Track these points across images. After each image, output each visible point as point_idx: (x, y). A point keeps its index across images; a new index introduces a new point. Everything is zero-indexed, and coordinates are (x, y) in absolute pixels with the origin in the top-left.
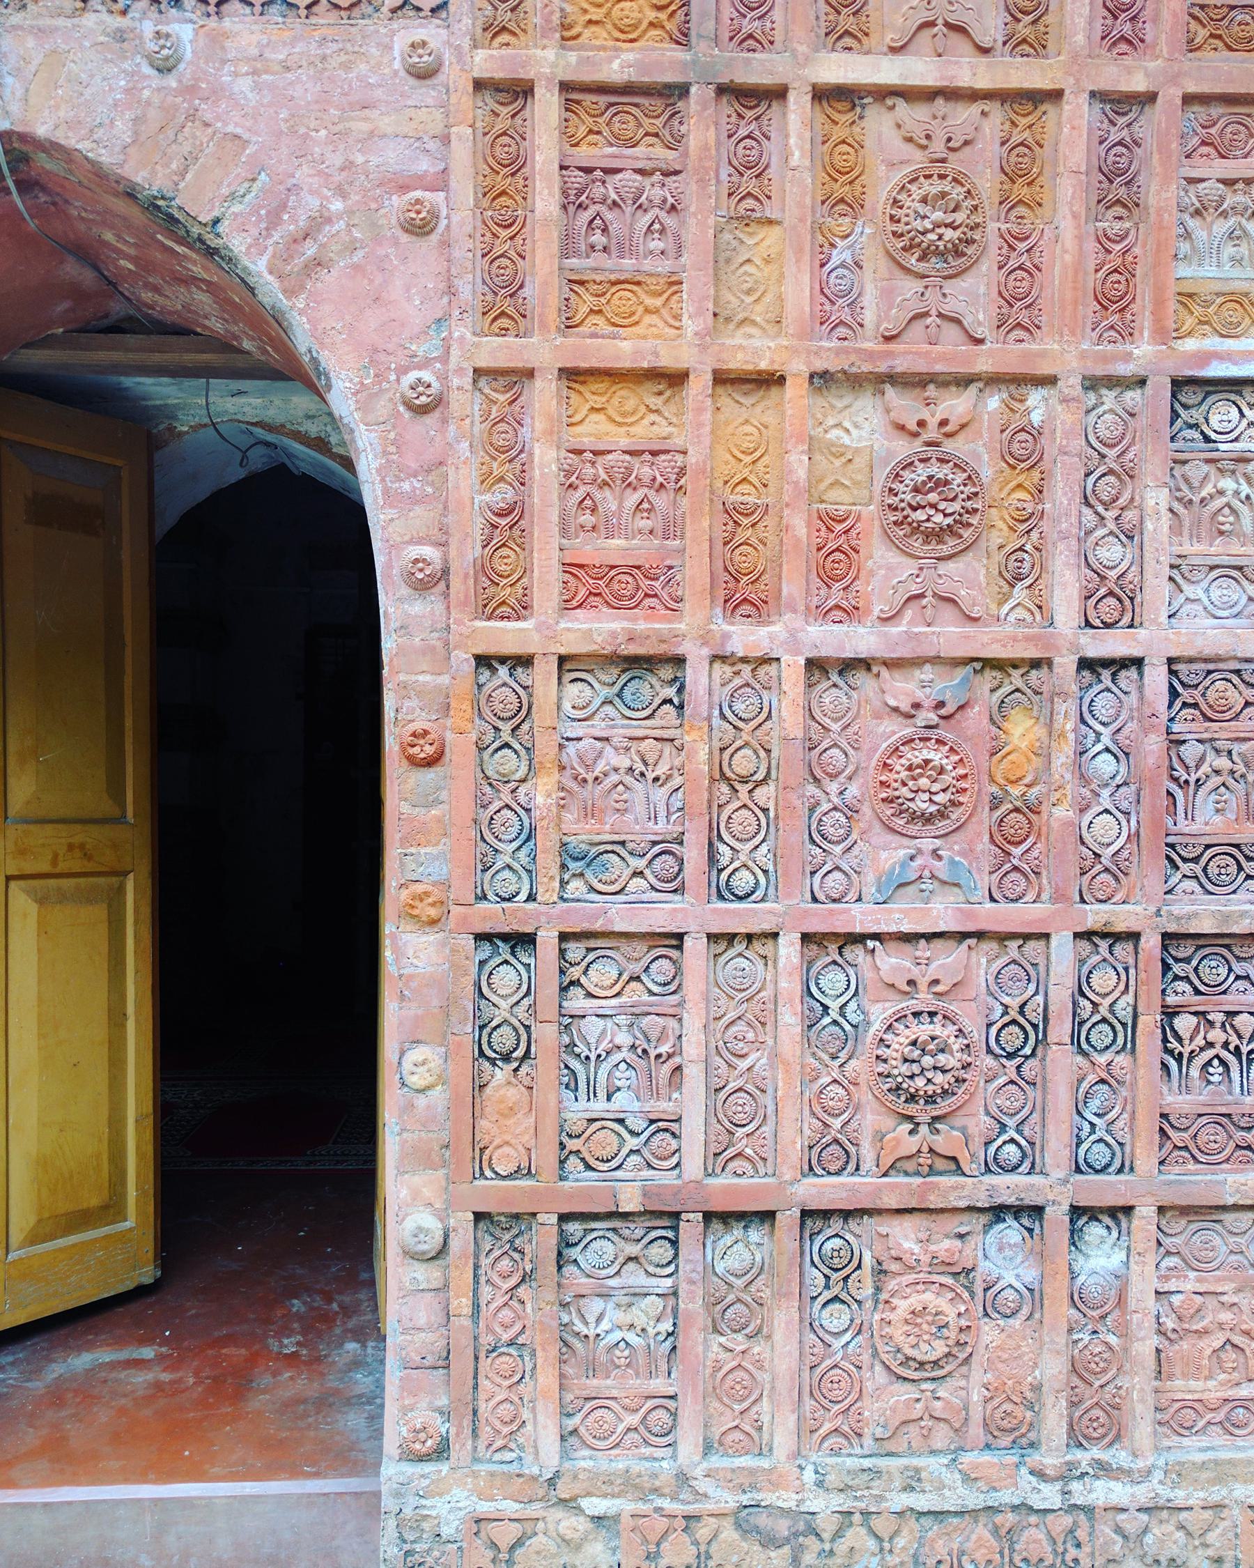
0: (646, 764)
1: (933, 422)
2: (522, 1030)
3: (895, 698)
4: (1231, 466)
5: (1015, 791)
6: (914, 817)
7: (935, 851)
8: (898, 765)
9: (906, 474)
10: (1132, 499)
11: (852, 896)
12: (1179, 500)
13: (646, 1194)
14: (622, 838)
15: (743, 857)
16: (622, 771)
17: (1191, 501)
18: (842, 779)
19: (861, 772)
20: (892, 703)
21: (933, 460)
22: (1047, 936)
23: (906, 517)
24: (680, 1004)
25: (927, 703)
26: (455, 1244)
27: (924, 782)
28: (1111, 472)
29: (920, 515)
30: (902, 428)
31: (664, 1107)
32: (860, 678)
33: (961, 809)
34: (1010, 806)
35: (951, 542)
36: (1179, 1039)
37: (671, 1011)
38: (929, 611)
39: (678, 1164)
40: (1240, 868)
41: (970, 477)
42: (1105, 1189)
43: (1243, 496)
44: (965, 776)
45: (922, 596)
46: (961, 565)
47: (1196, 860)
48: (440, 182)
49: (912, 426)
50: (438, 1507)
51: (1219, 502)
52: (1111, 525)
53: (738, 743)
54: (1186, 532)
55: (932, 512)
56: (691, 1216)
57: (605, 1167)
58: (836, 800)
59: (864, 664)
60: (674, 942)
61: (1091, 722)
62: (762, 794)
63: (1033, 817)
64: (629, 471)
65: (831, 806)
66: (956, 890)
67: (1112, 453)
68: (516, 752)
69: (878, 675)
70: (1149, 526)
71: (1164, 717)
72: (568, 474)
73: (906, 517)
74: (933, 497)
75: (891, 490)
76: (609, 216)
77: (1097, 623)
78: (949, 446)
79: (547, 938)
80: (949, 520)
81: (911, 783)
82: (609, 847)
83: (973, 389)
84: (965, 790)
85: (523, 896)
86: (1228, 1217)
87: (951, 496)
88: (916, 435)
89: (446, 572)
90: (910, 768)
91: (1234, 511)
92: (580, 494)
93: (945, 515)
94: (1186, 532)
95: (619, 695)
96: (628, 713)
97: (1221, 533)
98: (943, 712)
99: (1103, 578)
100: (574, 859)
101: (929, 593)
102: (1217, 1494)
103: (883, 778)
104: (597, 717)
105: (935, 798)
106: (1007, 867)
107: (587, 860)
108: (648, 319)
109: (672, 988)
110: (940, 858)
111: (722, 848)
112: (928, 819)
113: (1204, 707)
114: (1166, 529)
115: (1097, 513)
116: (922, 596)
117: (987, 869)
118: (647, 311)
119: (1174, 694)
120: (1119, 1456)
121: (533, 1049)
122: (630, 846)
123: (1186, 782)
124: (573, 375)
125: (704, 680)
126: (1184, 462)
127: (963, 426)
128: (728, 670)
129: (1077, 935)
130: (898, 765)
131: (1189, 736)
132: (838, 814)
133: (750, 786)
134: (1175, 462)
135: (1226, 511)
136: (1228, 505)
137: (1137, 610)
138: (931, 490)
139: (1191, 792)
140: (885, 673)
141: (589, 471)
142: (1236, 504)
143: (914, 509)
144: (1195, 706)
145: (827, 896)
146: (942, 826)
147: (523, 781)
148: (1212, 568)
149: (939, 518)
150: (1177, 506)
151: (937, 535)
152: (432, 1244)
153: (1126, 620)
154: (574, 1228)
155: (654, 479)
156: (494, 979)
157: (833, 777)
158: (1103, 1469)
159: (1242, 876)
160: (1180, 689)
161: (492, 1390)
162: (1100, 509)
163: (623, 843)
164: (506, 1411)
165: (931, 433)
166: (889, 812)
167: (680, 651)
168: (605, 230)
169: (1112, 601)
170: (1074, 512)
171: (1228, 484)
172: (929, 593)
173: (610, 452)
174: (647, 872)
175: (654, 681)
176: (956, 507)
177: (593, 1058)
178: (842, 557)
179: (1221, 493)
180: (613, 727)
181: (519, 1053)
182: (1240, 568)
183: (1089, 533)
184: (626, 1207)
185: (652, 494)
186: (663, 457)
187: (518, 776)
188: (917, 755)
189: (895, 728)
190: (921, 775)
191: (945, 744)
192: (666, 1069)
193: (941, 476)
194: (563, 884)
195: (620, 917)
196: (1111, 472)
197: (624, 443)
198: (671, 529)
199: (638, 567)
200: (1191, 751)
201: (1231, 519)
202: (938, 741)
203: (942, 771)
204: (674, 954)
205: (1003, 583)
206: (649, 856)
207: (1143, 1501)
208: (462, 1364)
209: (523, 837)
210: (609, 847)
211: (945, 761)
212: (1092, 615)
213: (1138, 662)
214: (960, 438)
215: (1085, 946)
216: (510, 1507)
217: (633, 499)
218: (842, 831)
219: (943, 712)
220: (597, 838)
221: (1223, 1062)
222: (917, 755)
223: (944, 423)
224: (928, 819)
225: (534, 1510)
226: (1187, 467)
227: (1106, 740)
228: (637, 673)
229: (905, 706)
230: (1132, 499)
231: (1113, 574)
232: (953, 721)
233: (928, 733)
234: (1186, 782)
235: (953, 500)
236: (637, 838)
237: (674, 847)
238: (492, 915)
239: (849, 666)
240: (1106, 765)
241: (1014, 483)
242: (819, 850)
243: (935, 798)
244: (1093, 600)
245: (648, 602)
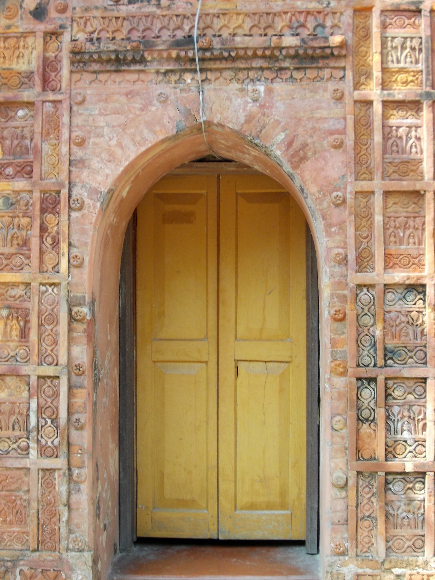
2: (372, 411)
13: (415, 466)
24: (426, 402)
26: (350, 482)
31: (420, 436)
37: (423, 404)
39: (425, 456)
48: (343, 132)
50: (345, 570)
56: (430, 473)
57: (401, 456)
60: (423, 381)
68: (369, 316)
76: (398, 141)
79: (381, 379)
82: (401, 348)
85: (372, 365)
89: (346, 256)
95: (404, 297)
100: (389, 354)
108: (412, 174)
109: (423, 396)
118: (412, 171)
121: (376, 416)
122: (408, 348)
124: (387, 194)
152: (342, 482)
154: (390, 477)
156: (363, 393)
161: (363, 534)
164: (366, 540)
167: (424, 282)
168: (397, 146)
173: (400, 217)
174: (414, 357)
177: (396, 420)
181: (371, 418)
184: (407, 470)
187: (370, 324)
192: (421, 424)
194: (386, 361)
195: (406, 373)
197: (404, 214)
199: (410, 255)
204: (423, 385)
206: (415, 351)
208: (352, 523)
210: (401, 348)
216: (369, 571)
220: (397, 345)
225: (377, 572)
237: (423, 349)
238: (363, 372)
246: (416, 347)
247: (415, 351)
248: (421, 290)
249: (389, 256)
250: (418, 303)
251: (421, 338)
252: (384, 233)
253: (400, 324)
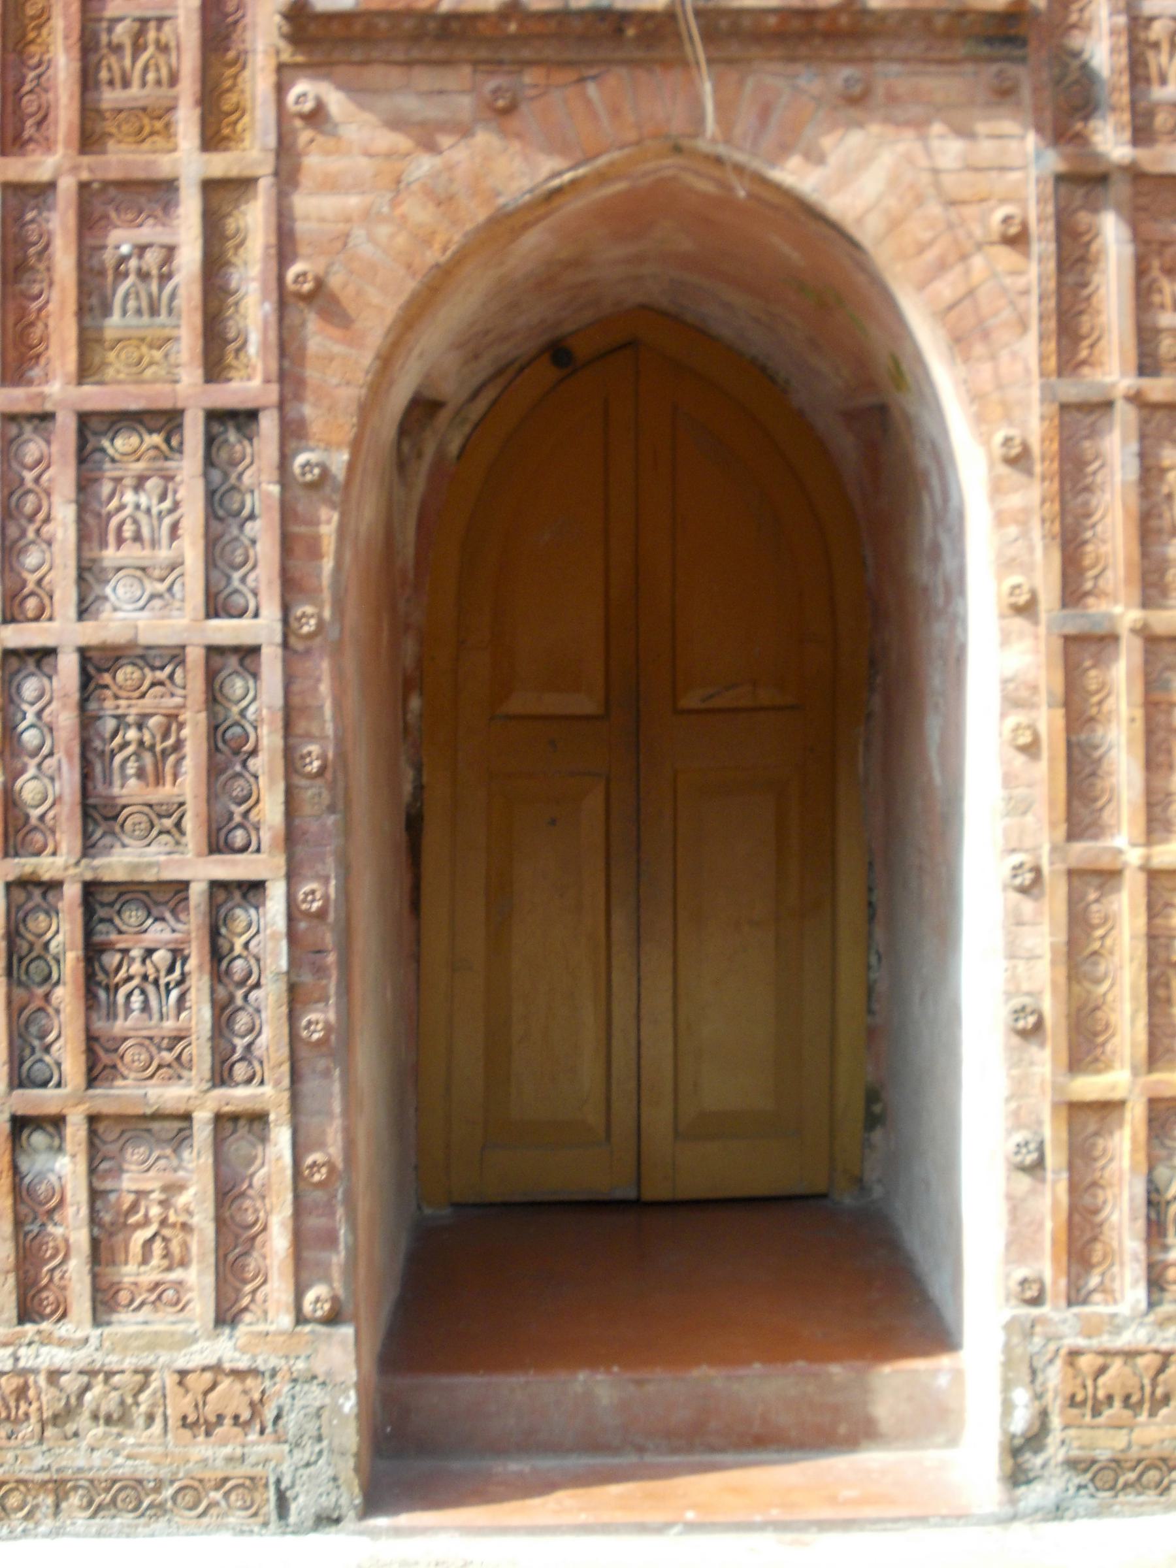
36: (106, 972)
42: (43, 1100)
86: (156, 1126)
102: (146, 1360)
120: (64, 1330)
158: (46, 1340)
182: (143, 569)
207: (82, 1365)
215: (19, 895)
221: (143, 992)
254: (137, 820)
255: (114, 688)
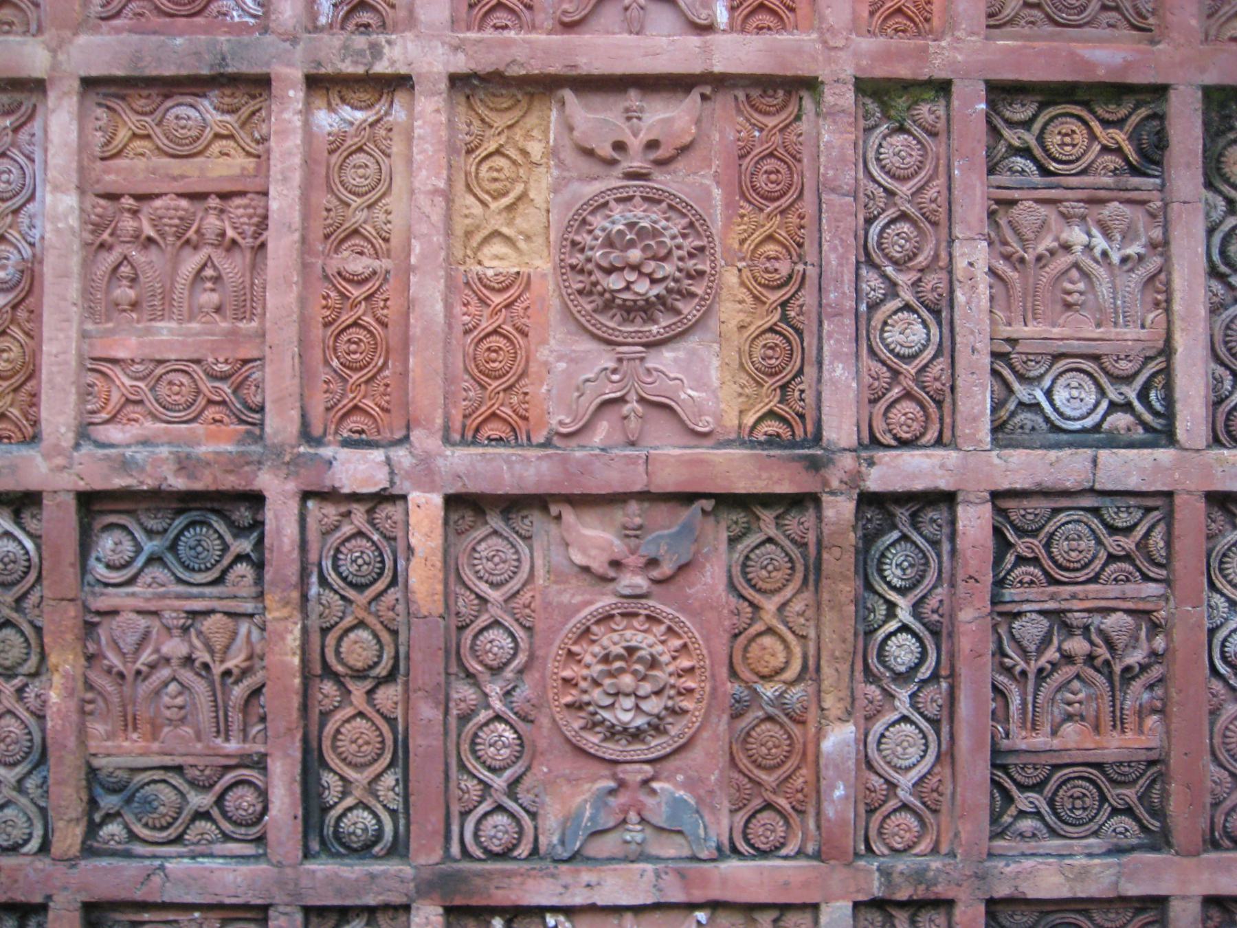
0: (212, 652)
1: (635, 144)
3: (584, 551)
4: (1080, 209)
5: (768, 691)
6: (613, 733)
7: (645, 782)
8: (590, 653)
9: (598, 221)
10: (936, 257)
11: (523, 850)
12: (1007, 258)
14: (178, 761)
15: (358, 793)
16: (174, 662)
17: (1022, 260)
18: (508, 674)
19: (537, 664)
20: (579, 559)
21: (637, 200)
22: (815, 907)
23: (595, 284)
25: (631, 560)
27: (627, 680)
28: (904, 216)
29: (615, 282)
30: (589, 153)
32: (535, 521)
33: (684, 720)
34: (761, 714)
35: (665, 320)
38: (633, 424)
40: (1103, 799)
41: (691, 224)
43: (1097, 252)
44: (691, 670)
45: (622, 400)
46: (681, 354)
47: (1038, 787)
49: (606, 150)
51: (1064, 260)
52: (907, 296)
53: (349, 621)
54: (1017, 305)
55: (632, 277)
58: (498, 705)
59: (539, 502)
61: (881, 587)
62: (388, 696)
63: (796, 730)
64: (186, 222)
65: (490, 713)
66: (679, 839)
67: (904, 189)
69: (558, 518)
70: (960, 297)
71: (989, 578)
72: (97, 228)
73: (595, 284)
74: (635, 255)
75: (574, 244)
77: (888, 439)
78: (663, 180)
80: (658, 289)
81: (607, 682)
82: (158, 775)
83: (695, 95)
84: (690, 691)
85: (34, 844)
87: (663, 252)
88: (612, 163)
90: (606, 659)
91: (1085, 275)
92: (111, 258)
93: (654, 282)
94: (1017, 305)
95: (173, 547)
96: (185, 576)
97: (1068, 306)
98: (655, 574)
99: (896, 373)
101: (633, 397)
103: (567, 673)
104: (140, 581)
105: (645, 706)
106: (757, 803)
107: (126, 793)
110: (653, 792)
111: (328, 778)
112: (637, 735)
113: (1047, 564)
114: (985, 303)
115: (885, 276)
116: (622, 400)
117: (726, 806)
119: (1002, 545)
123: (1024, 673)
125: (291, 530)
126: (1013, 203)
127: (684, 149)
128: (331, 511)
129: (857, 905)
130: (590, 653)
131: (1026, 607)
132: (501, 727)
133: (368, 684)
134: (998, 202)
135: (1075, 274)
136: (1076, 265)
137: (948, 420)
138: (631, 244)
139: (1030, 688)
140: (569, 515)
141: (128, 224)
142: (1087, 262)
143: (609, 271)
144: (1035, 561)
145: (486, 850)
146: (657, 745)
147: (35, 675)
148: (1057, 357)
149: (642, 287)
150: (1001, 266)
151: (645, 309)
153: (931, 435)
155: (223, 234)
157: (496, 671)
159: (1107, 808)
160: (1011, 536)
162: (889, 270)
163: (179, 769)
165: (636, 163)
166: (577, 724)
169: (908, 406)
170: (849, 276)
171: (1077, 236)
172: (633, 397)
173: (158, 196)
175: (221, 527)
176: (668, 268)
178: (502, 342)
179: (1067, 248)
180: (163, 596)
183: (873, 306)
185: (218, 256)
186: (238, 201)
188: (612, 640)
189: (587, 597)
190: (621, 671)
191: (660, 622)
193: (645, 223)
194: (92, 829)
196: (904, 216)
198: (246, 303)
200: (1031, 628)
201: (1081, 286)
202: (649, 618)
203: (653, 663)
205: (743, 379)
206: (218, 788)
209: (35, 756)
211: (660, 648)
212: (879, 426)
213: (948, 499)
214: (680, 165)
217: (191, 262)
218: (505, 752)
219: (655, 574)
222: (612, 640)
223: (652, 145)
224: (637, 735)
226: (1014, 211)
227: (904, 614)
228: (194, 515)
229: (598, 564)
230: (936, 257)
231: (911, 369)
232: (672, 588)
233: (632, 606)
234: (1024, 673)
235: (664, 259)
236: (201, 762)
239: (513, 505)
240: (903, 651)
241: (758, 236)
242: (471, 784)
243: (645, 706)
244: (882, 405)
245: (211, 412)
246: (227, 768)
247: (218, 788)
248: (243, 515)
249: (105, 367)
250: (231, 576)
251: (245, 731)
252: (86, 264)
253: (153, 667)
254: (1077, 792)
255: (1047, 564)
